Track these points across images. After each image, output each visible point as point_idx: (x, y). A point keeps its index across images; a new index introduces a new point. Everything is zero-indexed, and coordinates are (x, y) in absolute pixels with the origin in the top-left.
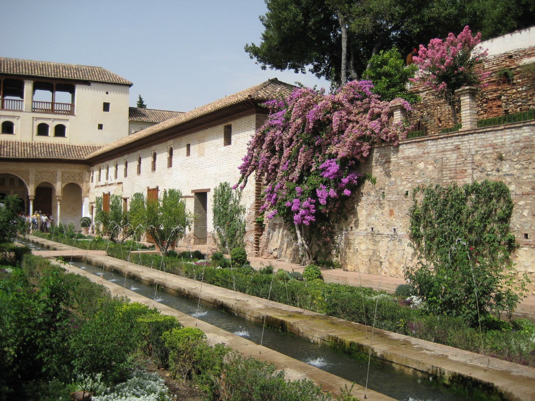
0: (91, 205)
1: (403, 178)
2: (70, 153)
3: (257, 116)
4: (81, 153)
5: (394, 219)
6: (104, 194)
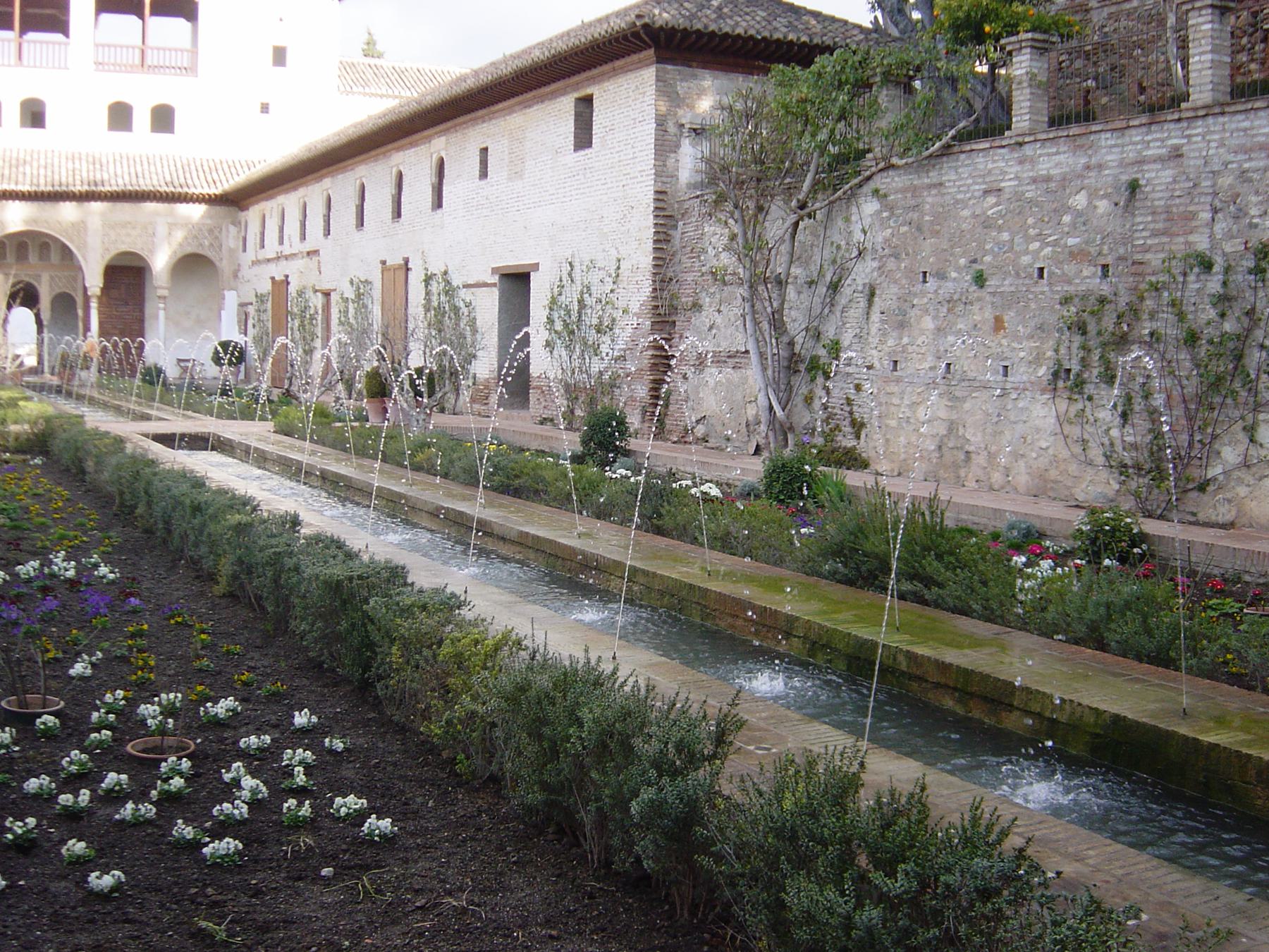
1: (1032, 232)
3: (657, 71)
4: (216, 177)
5: (1004, 342)
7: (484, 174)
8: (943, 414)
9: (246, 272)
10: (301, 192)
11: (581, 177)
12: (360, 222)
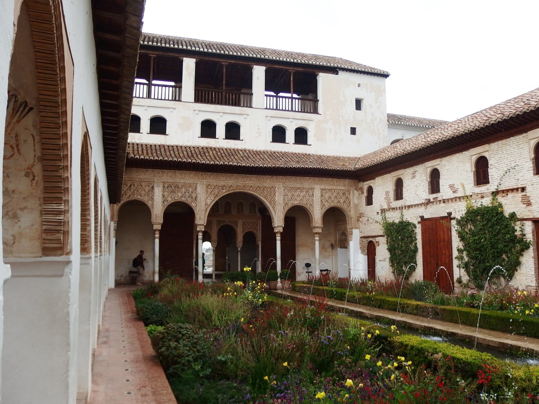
0: (366, 241)
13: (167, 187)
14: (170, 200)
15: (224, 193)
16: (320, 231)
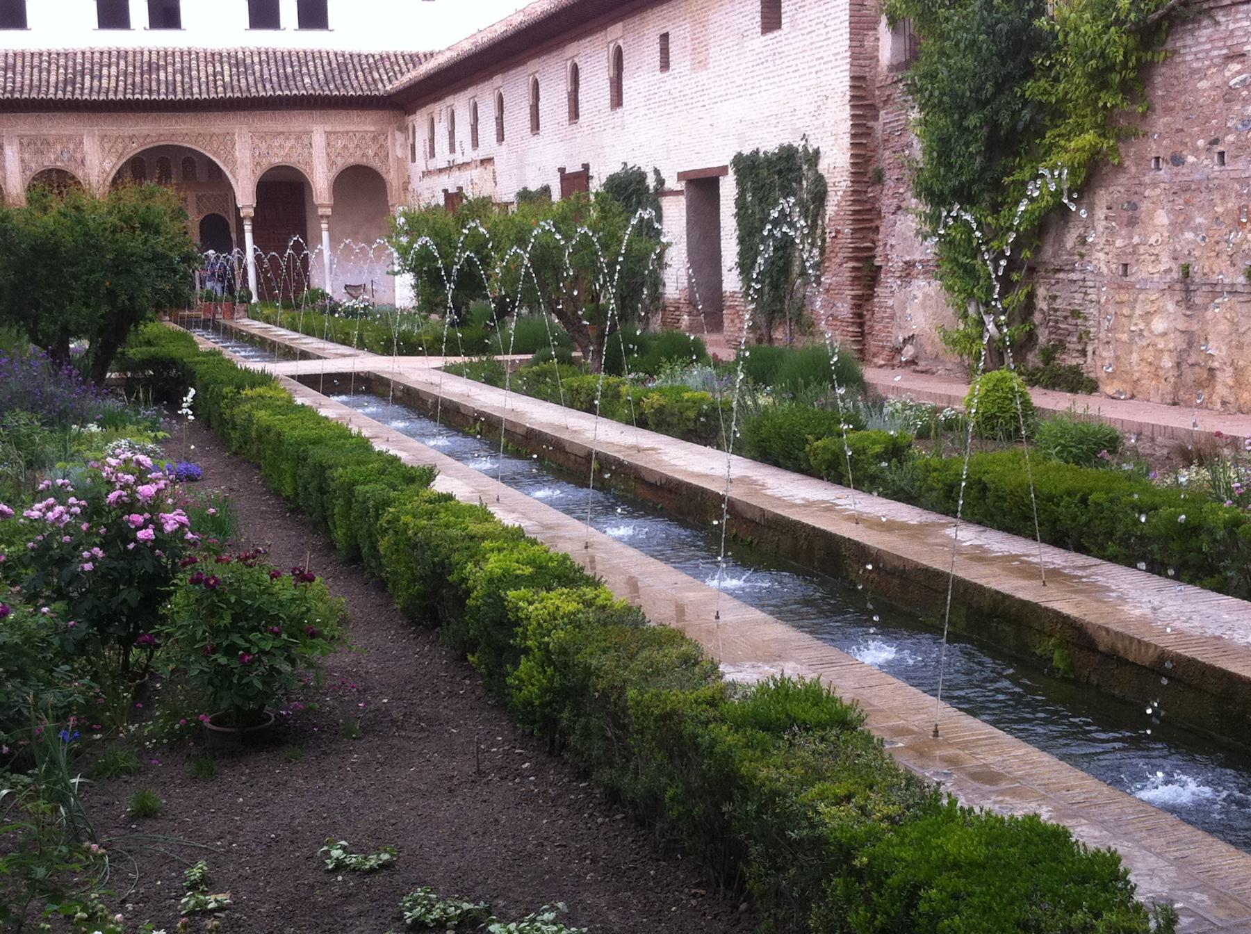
2: (345, 77)
4: (376, 76)
6: (448, 196)
7: (665, 65)
8: (1181, 325)
9: (416, 184)
10: (470, 92)
11: (769, 64)
12: (535, 126)
13: (26, 144)
14: (35, 167)
15: (135, 149)
16: (328, 211)
